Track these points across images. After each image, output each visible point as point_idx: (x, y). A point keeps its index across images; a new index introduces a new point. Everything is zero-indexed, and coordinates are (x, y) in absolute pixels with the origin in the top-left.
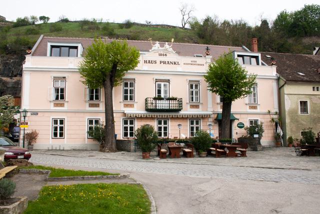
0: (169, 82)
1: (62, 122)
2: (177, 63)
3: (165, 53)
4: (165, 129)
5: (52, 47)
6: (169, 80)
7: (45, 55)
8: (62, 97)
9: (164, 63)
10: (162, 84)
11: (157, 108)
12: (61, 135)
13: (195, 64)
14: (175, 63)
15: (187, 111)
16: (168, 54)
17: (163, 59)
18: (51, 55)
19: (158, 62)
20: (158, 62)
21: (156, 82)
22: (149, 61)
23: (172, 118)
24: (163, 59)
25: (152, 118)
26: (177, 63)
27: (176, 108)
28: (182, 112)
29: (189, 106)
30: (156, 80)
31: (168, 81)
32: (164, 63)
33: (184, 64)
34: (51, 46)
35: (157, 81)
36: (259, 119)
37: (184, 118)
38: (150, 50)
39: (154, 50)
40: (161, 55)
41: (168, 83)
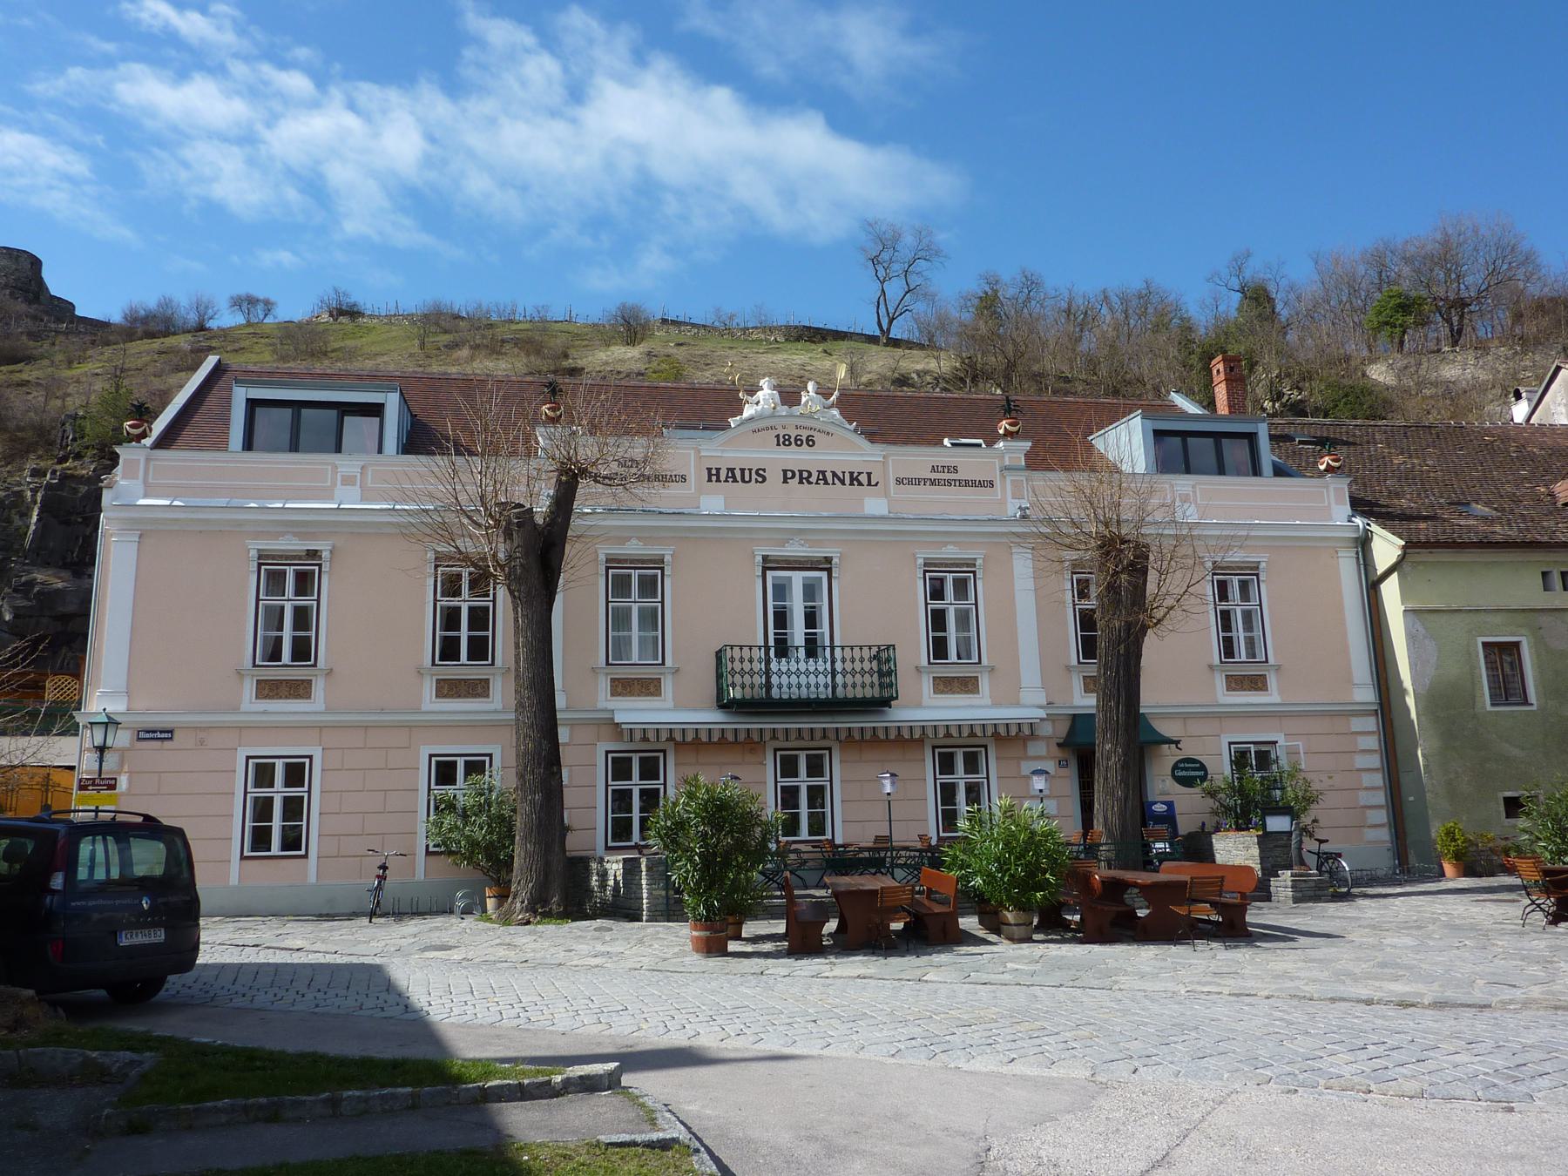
0: (829, 571)
1: (295, 774)
4: (816, 794)
5: (253, 404)
6: (828, 560)
7: (221, 444)
8: (302, 651)
9: (804, 478)
10: (797, 579)
11: (775, 693)
12: (292, 841)
13: (949, 483)
14: (854, 479)
15: (919, 706)
16: (818, 437)
18: (248, 445)
19: (774, 477)
20: (774, 477)
21: (765, 570)
22: (732, 470)
23: (855, 743)
25: (750, 745)
27: (869, 693)
28: (902, 714)
29: (927, 684)
30: (765, 558)
31: (825, 565)
32: (804, 478)
33: (899, 481)
34: (248, 400)
35: (768, 564)
36: (1282, 741)
37: (907, 741)
38: (733, 422)
39: (751, 419)
40: (784, 441)
41: (824, 575)
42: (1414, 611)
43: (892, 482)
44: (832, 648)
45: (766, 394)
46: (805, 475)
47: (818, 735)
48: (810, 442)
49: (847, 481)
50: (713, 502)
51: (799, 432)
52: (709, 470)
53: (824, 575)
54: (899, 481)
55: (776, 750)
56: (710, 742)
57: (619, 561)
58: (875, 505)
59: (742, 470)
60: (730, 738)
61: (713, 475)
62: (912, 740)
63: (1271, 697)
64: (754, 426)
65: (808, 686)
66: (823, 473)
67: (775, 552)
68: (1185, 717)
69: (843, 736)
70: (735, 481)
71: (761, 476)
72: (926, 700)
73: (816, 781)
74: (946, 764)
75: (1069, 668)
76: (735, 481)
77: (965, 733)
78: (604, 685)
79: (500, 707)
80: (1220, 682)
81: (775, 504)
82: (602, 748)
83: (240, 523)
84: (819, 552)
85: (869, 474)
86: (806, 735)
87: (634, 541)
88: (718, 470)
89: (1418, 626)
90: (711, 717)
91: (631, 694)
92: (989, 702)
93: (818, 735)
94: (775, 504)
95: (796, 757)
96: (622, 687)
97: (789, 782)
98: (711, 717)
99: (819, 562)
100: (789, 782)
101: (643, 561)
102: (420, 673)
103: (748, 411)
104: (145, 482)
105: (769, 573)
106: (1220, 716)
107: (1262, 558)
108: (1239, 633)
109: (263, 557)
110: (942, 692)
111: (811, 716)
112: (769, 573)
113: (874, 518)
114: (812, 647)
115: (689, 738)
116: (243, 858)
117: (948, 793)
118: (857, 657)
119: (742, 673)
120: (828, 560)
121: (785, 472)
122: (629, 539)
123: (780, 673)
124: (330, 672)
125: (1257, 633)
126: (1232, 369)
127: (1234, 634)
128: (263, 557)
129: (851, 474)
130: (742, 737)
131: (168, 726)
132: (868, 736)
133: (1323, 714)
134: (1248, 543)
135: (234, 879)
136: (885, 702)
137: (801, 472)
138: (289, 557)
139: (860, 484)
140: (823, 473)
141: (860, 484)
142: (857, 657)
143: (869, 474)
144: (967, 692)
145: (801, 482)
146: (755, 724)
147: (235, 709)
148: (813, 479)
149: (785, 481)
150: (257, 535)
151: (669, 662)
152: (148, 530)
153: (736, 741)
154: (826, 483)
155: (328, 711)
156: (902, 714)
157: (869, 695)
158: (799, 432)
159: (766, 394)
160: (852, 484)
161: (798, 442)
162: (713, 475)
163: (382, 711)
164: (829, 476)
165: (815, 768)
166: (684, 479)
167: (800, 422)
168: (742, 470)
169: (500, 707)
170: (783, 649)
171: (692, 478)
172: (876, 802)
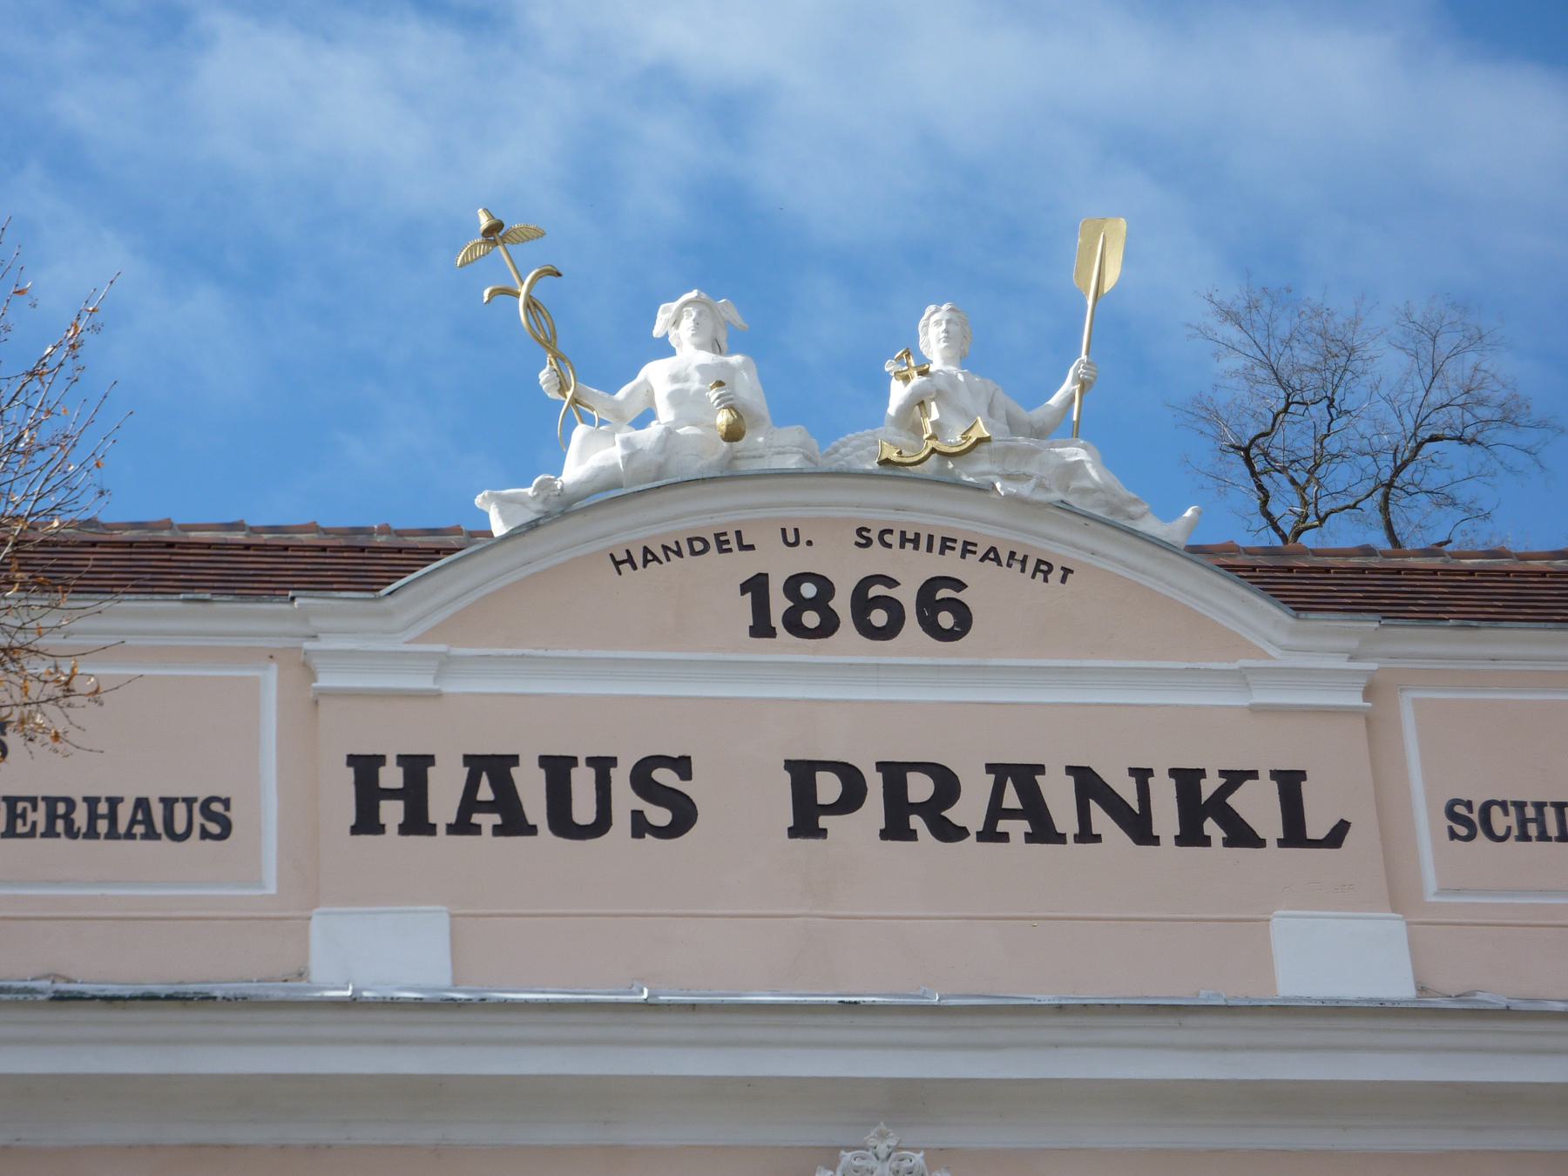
2: (1258, 805)
3: (910, 573)
9: (916, 803)
14: (1206, 810)
16: (984, 588)
17: (870, 698)
19: (741, 799)
20: (741, 799)
22: (497, 767)
24: (870, 698)
26: (1258, 805)
32: (916, 803)
33: (1467, 821)
39: (607, 494)
40: (797, 610)
43: (1427, 824)
46: (920, 788)
48: (945, 612)
50: (390, 934)
51: (877, 560)
52: (365, 767)
54: (1467, 821)
58: (1330, 944)
59: (557, 769)
61: (385, 794)
66: (1025, 776)
76: (514, 824)
85: (1290, 784)
121: (802, 773)
129: (1188, 780)
137: (894, 774)
139: (1241, 835)
140: (1025, 776)
141: (1241, 835)
143: (1290, 784)
145: (896, 829)
148: (969, 811)
149: (806, 822)
158: (877, 560)
160: (1191, 836)
161: (875, 612)
162: (385, 794)
166: (216, 819)
171: (264, 815)
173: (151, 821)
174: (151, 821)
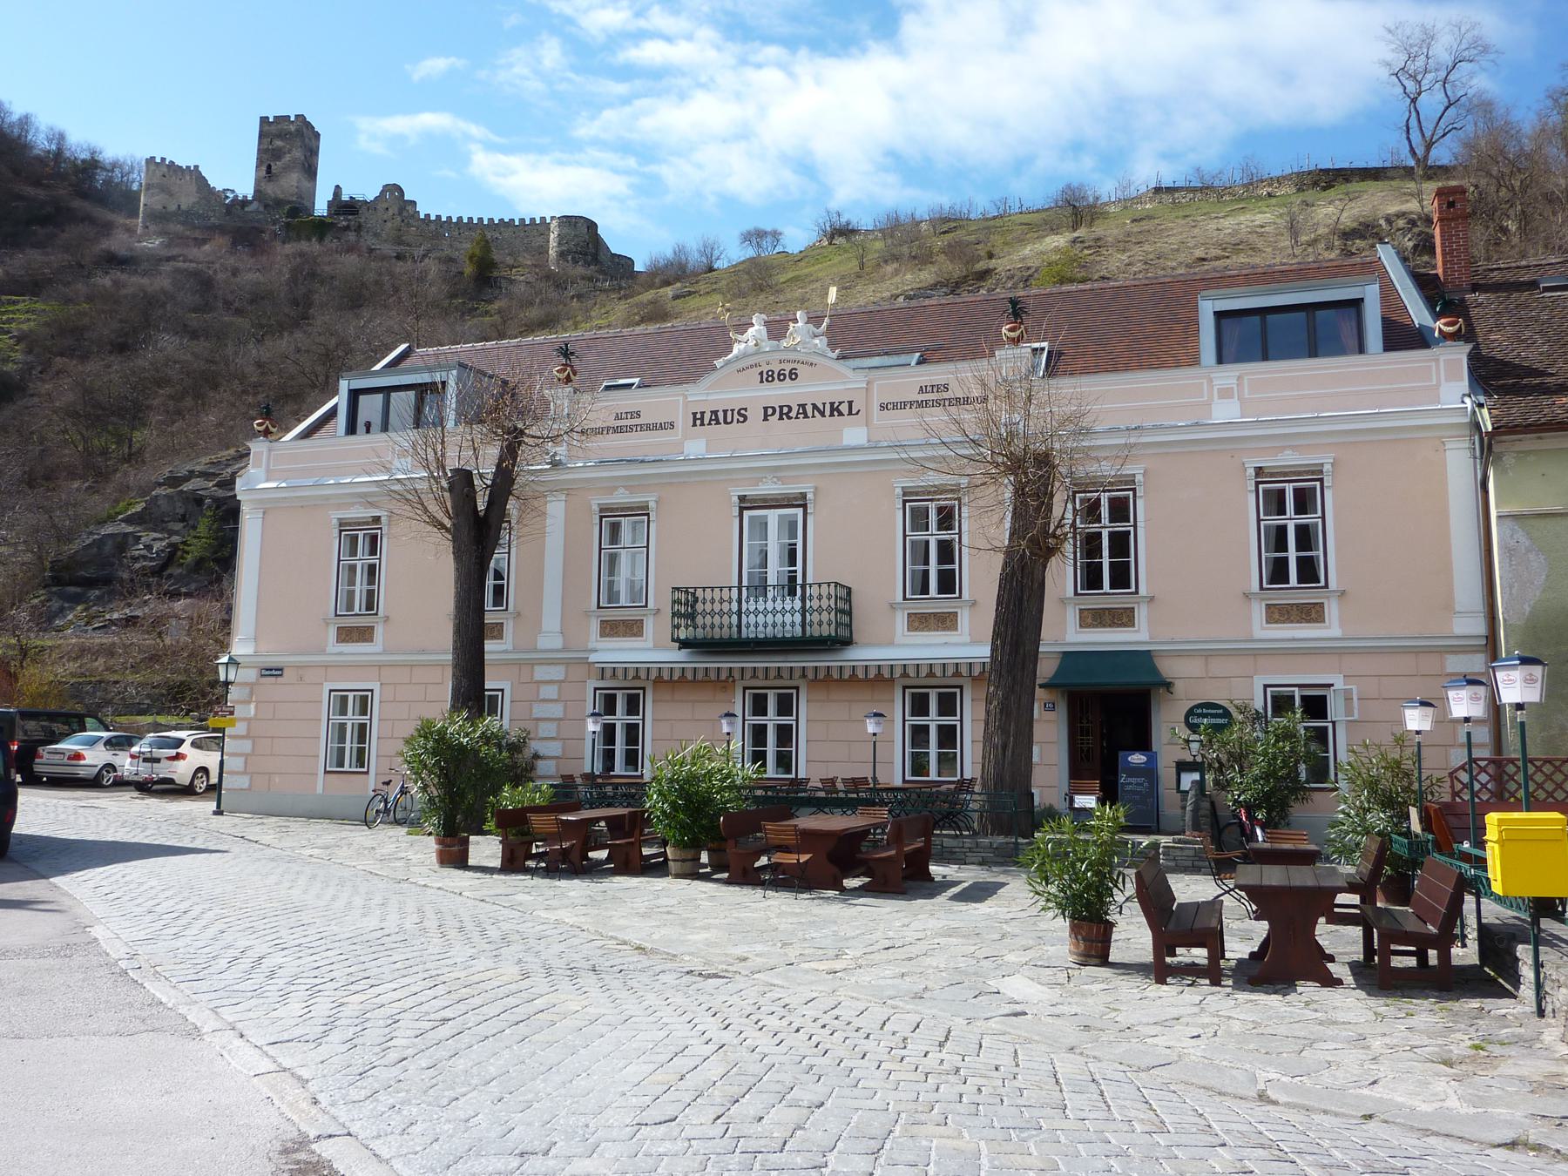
0: (804, 506)
1: (364, 705)
2: (844, 408)
3: (788, 367)
4: (785, 734)
6: (804, 496)
9: (784, 413)
10: (773, 516)
11: (744, 635)
13: (630, 429)
14: (835, 410)
15: (891, 643)
16: (802, 370)
17: (780, 393)
19: (755, 414)
20: (755, 414)
21: (742, 509)
22: (715, 413)
23: (825, 681)
24: (780, 393)
25: (723, 683)
26: (844, 408)
27: (826, 631)
28: (862, 654)
29: (901, 620)
30: (742, 499)
31: (801, 501)
32: (784, 413)
33: (883, 407)
35: (745, 503)
36: (1339, 683)
37: (878, 680)
38: (719, 363)
39: (737, 358)
40: (768, 377)
41: (800, 511)
42: (1515, 517)
43: (876, 407)
44: (803, 587)
45: (757, 330)
46: (785, 410)
47: (772, 674)
48: (793, 375)
49: (827, 412)
50: (695, 446)
51: (782, 366)
52: (694, 414)
53: (800, 511)
54: (883, 407)
55: (905, 688)
56: (841, 680)
57: (612, 510)
58: (853, 434)
59: (725, 412)
60: (689, 676)
61: (698, 419)
62: (841, 680)
63: (1331, 629)
64: (740, 365)
65: (784, 624)
66: (803, 406)
67: (749, 492)
68: (1208, 655)
69: (811, 675)
70: (718, 423)
71: (743, 416)
72: (899, 639)
73: (785, 720)
74: (920, 706)
75: (1247, 596)
76: (718, 423)
77: (950, 672)
78: (595, 626)
79: (510, 647)
80: (1258, 611)
81: (757, 442)
82: (593, 683)
83: (327, 497)
84: (793, 489)
85: (850, 403)
86: (785, 674)
87: (622, 490)
88: (703, 413)
89: (1520, 535)
90: (674, 656)
91: (617, 634)
92: (967, 639)
93: (772, 674)
94: (757, 442)
95: (927, 695)
96: (611, 629)
97: (920, 720)
98: (674, 656)
99: (795, 499)
100: (920, 720)
101: (632, 509)
102: (387, 618)
103: (737, 349)
104: (268, 470)
105: (746, 514)
106: (1255, 654)
107: (1325, 459)
108: (360, 587)
109: (342, 524)
110: (916, 630)
111: (770, 656)
112: (746, 514)
113: (854, 448)
114: (791, 586)
115: (872, 675)
116: (326, 772)
117: (920, 734)
118: (717, 598)
119: (712, 614)
120: (804, 496)
121: (766, 409)
122: (616, 488)
123: (793, 612)
124: (387, 618)
125: (344, 588)
126: (1451, 205)
127: (365, 587)
128: (342, 524)
129: (832, 404)
130: (700, 676)
131: (279, 665)
132: (821, 676)
133: (1417, 651)
134: (1134, 451)
135: (320, 790)
136: (843, 642)
137: (781, 407)
138: (359, 523)
139: (840, 414)
140: (803, 406)
141: (840, 414)
142: (717, 598)
143: (850, 403)
144: (944, 629)
145: (781, 418)
146: (725, 663)
147: (323, 652)
148: (793, 414)
149: (765, 419)
150: (339, 507)
151: (651, 605)
152: (268, 508)
153: (695, 680)
154: (806, 416)
155: (385, 652)
156: (862, 654)
157: (825, 634)
158: (782, 366)
159: (757, 330)
160: (832, 415)
161: (781, 376)
162: (698, 419)
163: (423, 652)
164: (809, 409)
165: (785, 707)
166: (672, 425)
167: (784, 356)
168: (725, 412)
169: (510, 647)
170: (760, 588)
171: (679, 425)
172: (850, 743)
173: (662, 427)
174: (662, 427)
